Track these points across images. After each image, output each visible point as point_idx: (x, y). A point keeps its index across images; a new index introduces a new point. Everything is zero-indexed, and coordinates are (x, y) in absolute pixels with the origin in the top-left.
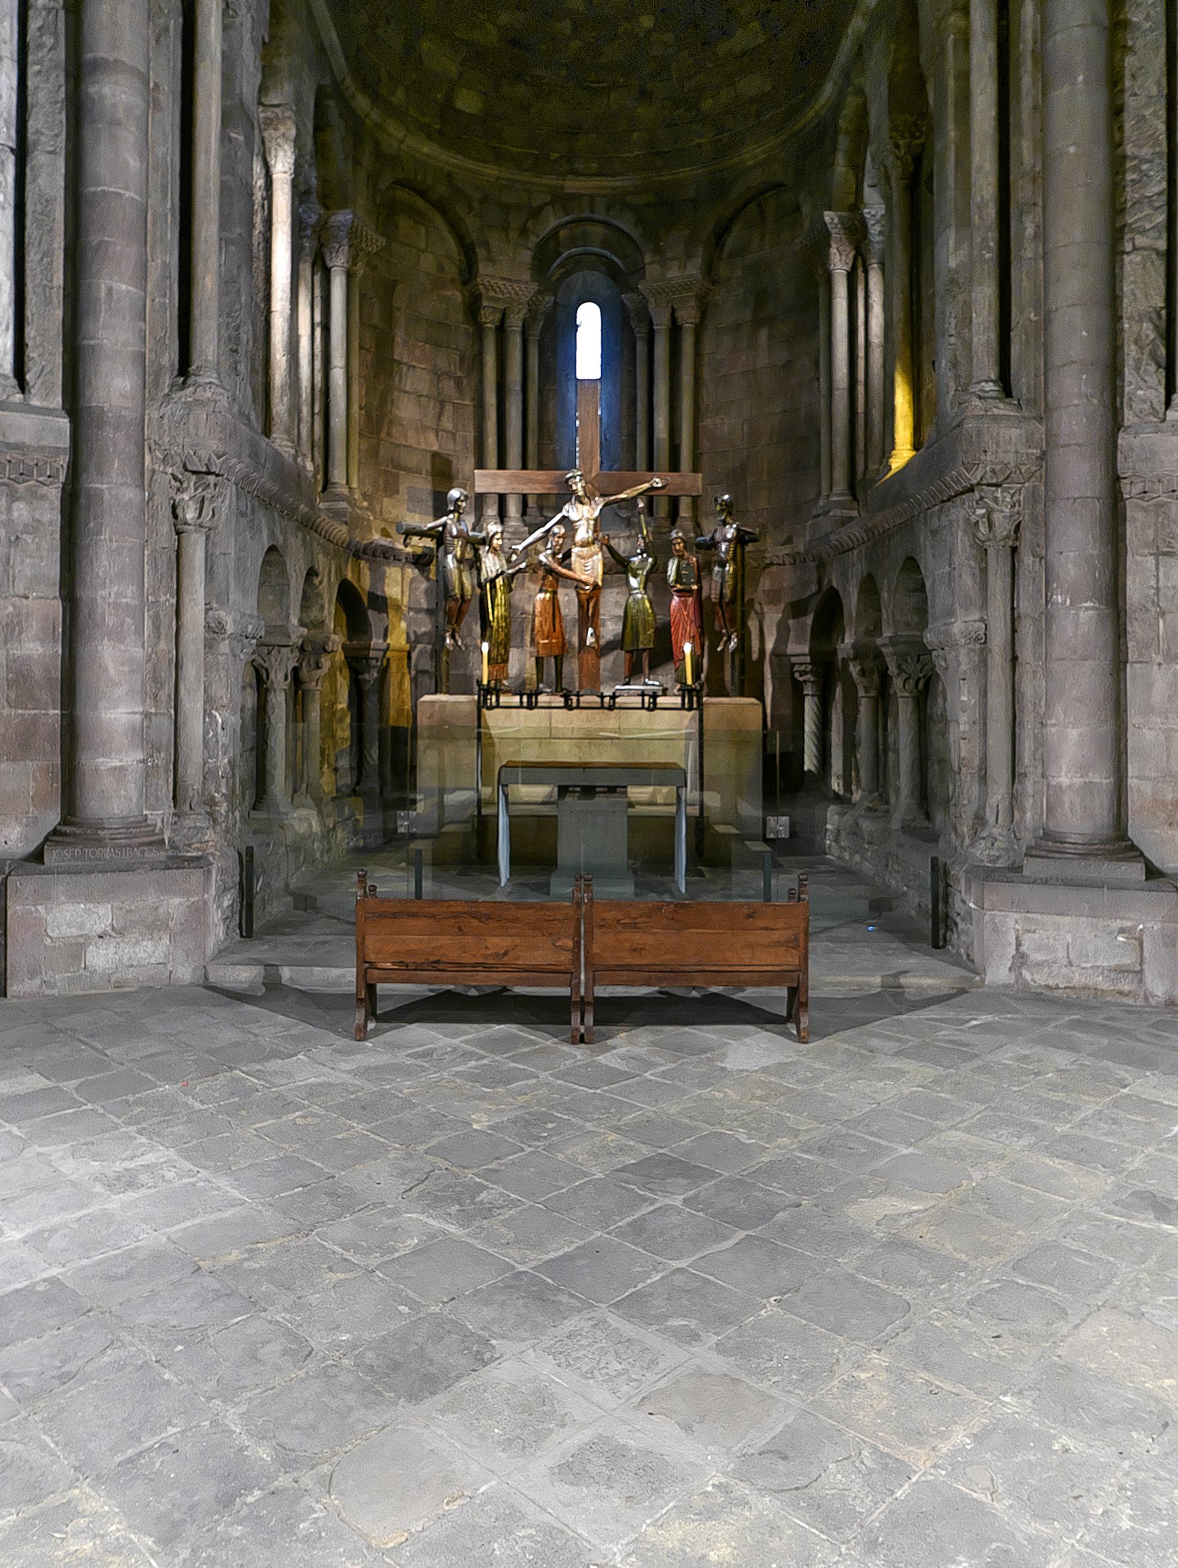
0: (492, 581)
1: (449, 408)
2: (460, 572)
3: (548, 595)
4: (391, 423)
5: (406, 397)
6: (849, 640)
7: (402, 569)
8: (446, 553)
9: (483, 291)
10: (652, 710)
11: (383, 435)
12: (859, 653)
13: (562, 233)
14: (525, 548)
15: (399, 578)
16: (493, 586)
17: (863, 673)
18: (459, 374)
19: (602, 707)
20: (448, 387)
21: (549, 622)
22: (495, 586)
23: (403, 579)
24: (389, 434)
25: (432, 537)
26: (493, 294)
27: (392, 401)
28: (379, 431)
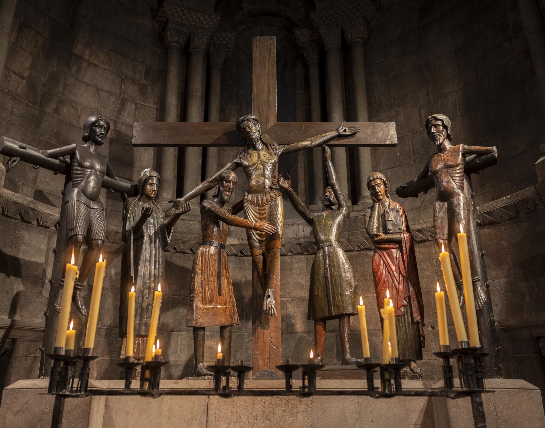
0: (138, 230)
4: (61, 102)
5: (83, 88)
11: (49, 109)
16: (139, 238)
18: (143, 81)
19: (289, 390)
21: (213, 284)
24: (56, 111)
25: (55, 169)
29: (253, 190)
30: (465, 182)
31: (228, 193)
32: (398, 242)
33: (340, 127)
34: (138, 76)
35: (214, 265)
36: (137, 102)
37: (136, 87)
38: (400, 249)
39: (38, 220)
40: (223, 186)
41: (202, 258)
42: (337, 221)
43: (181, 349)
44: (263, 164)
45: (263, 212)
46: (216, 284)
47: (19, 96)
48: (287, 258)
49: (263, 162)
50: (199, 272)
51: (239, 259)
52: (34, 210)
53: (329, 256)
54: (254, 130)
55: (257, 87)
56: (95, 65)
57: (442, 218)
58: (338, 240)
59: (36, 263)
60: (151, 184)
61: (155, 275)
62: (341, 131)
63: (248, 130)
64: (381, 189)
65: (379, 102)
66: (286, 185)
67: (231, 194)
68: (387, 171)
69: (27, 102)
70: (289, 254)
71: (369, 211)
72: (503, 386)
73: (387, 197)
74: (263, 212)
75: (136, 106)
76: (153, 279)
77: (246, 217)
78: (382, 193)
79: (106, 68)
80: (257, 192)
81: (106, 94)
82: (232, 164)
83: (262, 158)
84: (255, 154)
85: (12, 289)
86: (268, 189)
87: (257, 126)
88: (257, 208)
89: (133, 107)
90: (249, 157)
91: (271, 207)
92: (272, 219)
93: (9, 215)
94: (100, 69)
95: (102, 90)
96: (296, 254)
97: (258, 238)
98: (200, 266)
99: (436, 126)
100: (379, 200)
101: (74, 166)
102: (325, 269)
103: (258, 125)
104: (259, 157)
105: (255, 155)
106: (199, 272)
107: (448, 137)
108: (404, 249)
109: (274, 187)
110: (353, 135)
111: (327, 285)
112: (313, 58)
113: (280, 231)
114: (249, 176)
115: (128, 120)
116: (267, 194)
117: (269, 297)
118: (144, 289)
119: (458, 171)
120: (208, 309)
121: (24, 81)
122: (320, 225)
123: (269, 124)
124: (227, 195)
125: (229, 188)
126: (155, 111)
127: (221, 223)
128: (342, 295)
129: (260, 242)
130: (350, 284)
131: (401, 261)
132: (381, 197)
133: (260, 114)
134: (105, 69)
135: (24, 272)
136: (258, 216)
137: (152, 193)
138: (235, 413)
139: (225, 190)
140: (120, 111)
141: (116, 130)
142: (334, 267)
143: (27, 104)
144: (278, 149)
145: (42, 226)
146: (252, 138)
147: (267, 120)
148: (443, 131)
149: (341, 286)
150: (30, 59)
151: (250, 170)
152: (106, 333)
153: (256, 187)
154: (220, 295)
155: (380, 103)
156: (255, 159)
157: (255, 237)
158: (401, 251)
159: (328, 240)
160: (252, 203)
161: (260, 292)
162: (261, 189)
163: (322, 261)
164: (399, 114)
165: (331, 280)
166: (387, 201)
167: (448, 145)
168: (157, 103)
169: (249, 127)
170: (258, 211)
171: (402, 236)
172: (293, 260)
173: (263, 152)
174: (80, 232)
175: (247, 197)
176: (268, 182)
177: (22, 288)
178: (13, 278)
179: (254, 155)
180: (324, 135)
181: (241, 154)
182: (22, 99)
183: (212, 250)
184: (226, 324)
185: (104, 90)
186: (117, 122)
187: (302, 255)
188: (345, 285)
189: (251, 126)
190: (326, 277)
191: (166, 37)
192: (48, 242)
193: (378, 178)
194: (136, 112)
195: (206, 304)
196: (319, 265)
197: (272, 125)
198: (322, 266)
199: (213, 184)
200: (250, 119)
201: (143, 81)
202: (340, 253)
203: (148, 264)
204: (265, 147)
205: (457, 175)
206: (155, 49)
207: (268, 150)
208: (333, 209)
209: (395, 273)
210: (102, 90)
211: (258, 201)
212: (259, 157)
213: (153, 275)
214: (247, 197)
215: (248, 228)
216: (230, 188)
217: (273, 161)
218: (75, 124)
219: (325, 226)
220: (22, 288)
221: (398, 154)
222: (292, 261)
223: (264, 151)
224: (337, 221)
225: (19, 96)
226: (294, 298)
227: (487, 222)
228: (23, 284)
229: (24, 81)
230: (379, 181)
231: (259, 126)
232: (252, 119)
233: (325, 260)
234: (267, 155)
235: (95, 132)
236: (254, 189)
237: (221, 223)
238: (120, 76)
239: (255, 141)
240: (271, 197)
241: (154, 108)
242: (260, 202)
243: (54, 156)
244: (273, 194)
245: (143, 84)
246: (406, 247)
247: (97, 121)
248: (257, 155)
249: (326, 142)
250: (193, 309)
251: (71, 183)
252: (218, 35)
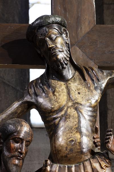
29: (62, 157)
31: (17, 162)
40: (9, 149)
49: (78, 103)
63: (51, 45)
67: (23, 162)
80: (69, 159)
82: (21, 105)
83: (75, 95)
84: (61, 86)
86: (87, 155)
87: (64, 35)
90: (51, 94)
103: (67, 33)
104: (69, 93)
105: (63, 90)
109: (97, 150)
116: (87, 164)
123: (81, 28)
124: (16, 165)
125: (19, 152)
133: (65, 9)
139: (12, 157)
144: (100, 78)
146: (57, 58)
147: (78, 21)
151: (55, 118)
153: (67, 152)
156: (63, 99)
169: (51, 39)
173: (76, 84)
175: (51, 167)
176: (86, 142)
179: (60, 90)
181: (37, 87)
189: (54, 36)
197: (88, 30)
200: (53, 23)
204: (77, 73)
207: (85, 80)
212: (69, 93)
214: (51, 167)
216: (21, 153)
217: (93, 102)
223: (78, 82)
231: (67, 36)
232: (57, 23)
234: (83, 90)
236: (64, 155)
239: (62, 64)
244: (96, 165)
248: (65, 90)
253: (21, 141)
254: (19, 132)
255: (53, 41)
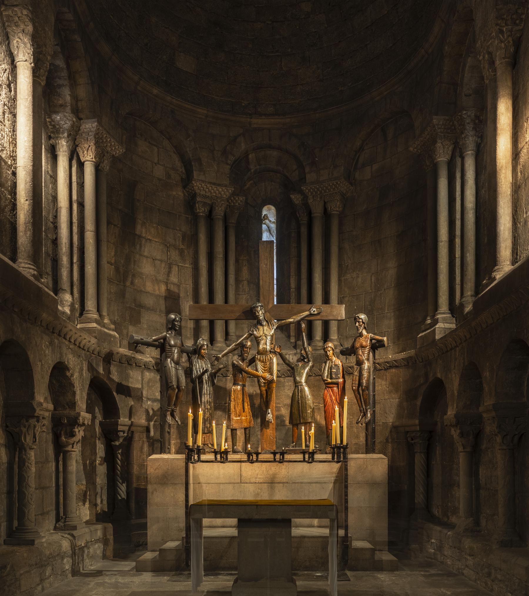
0: (200, 377)
1: (175, 269)
2: (177, 369)
3: (239, 387)
4: (134, 276)
6: (451, 412)
7: (142, 373)
8: (167, 357)
9: (198, 191)
10: (311, 463)
11: (128, 283)
12: (459, 421)
13: (250, 156)
14: (223, 356)
15: (140, 378)
16: (201, 382)
17: (462, 435)
18: (182, 247)
19: (275, 461)
20: (174, 255)
22: (202, 381)
23: (142, 379)
24: (132, 283)
25: (156, 347)
26: (203, 193)
27: (135, 261)
28: (125, 280)
30: (371, 354)
32: (337, 384)
33: (311, 308)
34: (177, 242)
35: (240, 396)
36: (179, 264)
37: (177, 252)
38: (338, 387)
39: (136, 363)
40: (244, 351)
41: (234, 393)
42: (306, 371)
43: (219, 435)
44: (266, 336)
45: (266, 366)
46: (242, 407)
47: (112, 279)
48: (282, 379)
50: (233, 400)
51: (252, 379)
52: (134, 358)
53: (301, 392)
54: (261, 313)
55: (262, 280)
56: (150, 240)
57: (356, 375)
58: (306, 382)
59: (137, 388)
60: (204, 349)
61: (210, 401)
62: (312, 312)
63: (257, 314)
64: (330, 353)
65: (347, 265)
66: (279, 351)
68: (348, 320)
69: (116, 282)
70: (283, 376)
71: (324, 364)
72: (372, 457)
73: (334, 356)
74: (266, 366)
75: (178, 268)
76: (209, 403)
77: (257, 370)
78: (331, 355)
79: (157, 241)
81: (159, 262)
83: (265, 332)
84: (261, 328)
85: (128, 404)
88: (263, 363)
89: (177, 269)
91: (270, 363)
92: (270, 371)
93: (123, 362)
94: (153, 242)
95: (156, 259)
96: (287, 377)
97: (263, 381)
98: (233, 397)
99: (359, 322)
100: (329, 359)
101: (166, 346)
102: (298, 398)
106: (233, 400)
107: (365, 328)
108: (340, 388)
109: (272, 351)
110: (318, 314)
111: (299, 407)
112: (304, 220)
113: (275, 378)
114: (258, 343)
115: (174, 280)
116: (268, 355)
117: (269, 413)
118: (205, 409)
119: (367, 350)
120: (238, 420)
121: (113, 266)
122: (297, 372)
124: (246, 356)
126: (191, 270)
127: (243, 373)
128: (306, 413)
129: (264, 383)
130: (311, 407)
131: (338, 394)
132: (330, 358)
134: (156, 242)
135: (132, 394)
136: (263, 368)
137: (204, 355)
138: (253, 469)
140: (169, 273)
141: (167, 289)
142: (303, 397)
143: (116, 283)
144: (274, 325)
145: (138, 366)
148: (362, 325)
149: (306, 408)
150: (114, 249)
151: (259, 340)
152: (177, 427)
154: (244, 412)
155: (347, 265)
156: (261, 333)
157: (262, 381)
158: (338, 389)
159: (301, 382)
160: (260, 360)
161: (264, 409)
162: (264, 352)
163: (297, 394)
164: (358, 277)
165: (301, 404)
166: (334, 359)
167: (364, 332)
168: (192, 263)
169: (258, 312)
170: (263, 365)
171: (339, 381)
172: (285, 380)
174: (175, 384)
176: (268, 348)
177: (133, 403)
178: (128, 397)
180: (301, 314)
182: (113, 280)
183: (239, 387)
184: (247, 427)
185: (157, 259)
186: (167, 283)
187: (291, 377)
188: (308, 407)
190: (299, 403)
191: (195, 208)
192: (142, 375)
193: (329, 347)
194: (179, 273)
195: (237, 417)
196: (295, 396)
197: (271, 306)
198: (297, 397)
199: (237, 346)
200: (258, 306)
201: (182, 247)
202: (306, 389)
203: (206, 396)
205: (366, 352)
206: (187, 216)
208: (305, 361)
209: (334, 401)
210: (156, 259)
211: (263, 360)
213: (209, 401)
215: (258, 377)
217: (271, 334)
218: (143, 290)
219: (299, 373)
220: (133, 403)
221: (355, 308)
222: (285, 381)
224: (306, 371)
225: (112, 279)
226: (285, 404)
227: (394, 366)
228: (133, 401)
229: (113, 266)
230: (329, 349)
232: (260, 306)
233: (298, 393)
234: (268, 329)
235: (175, 325)
237: (243, 373)
238: (166, 245)
240: (270, 358)
241: (190, 267)
242: (264, 360)
243: (155, 340)
244: (271, 356)
245: (182, 248)
246: (341, 386)
247: (175, 318)
248: (262, 330)
249: (302, 319)
250: (230, 420)
251: (164, 354)
252: (232, 198)
253: (247, 348)
254: (247, 345)
255: (258, 312)
